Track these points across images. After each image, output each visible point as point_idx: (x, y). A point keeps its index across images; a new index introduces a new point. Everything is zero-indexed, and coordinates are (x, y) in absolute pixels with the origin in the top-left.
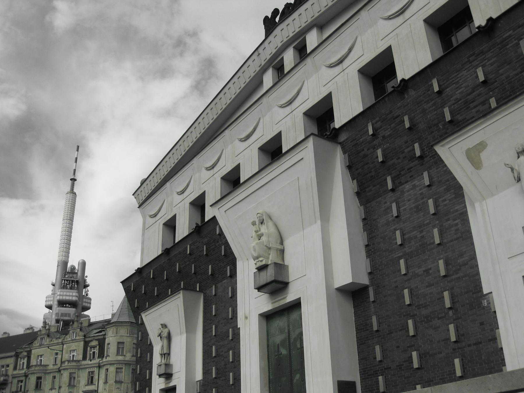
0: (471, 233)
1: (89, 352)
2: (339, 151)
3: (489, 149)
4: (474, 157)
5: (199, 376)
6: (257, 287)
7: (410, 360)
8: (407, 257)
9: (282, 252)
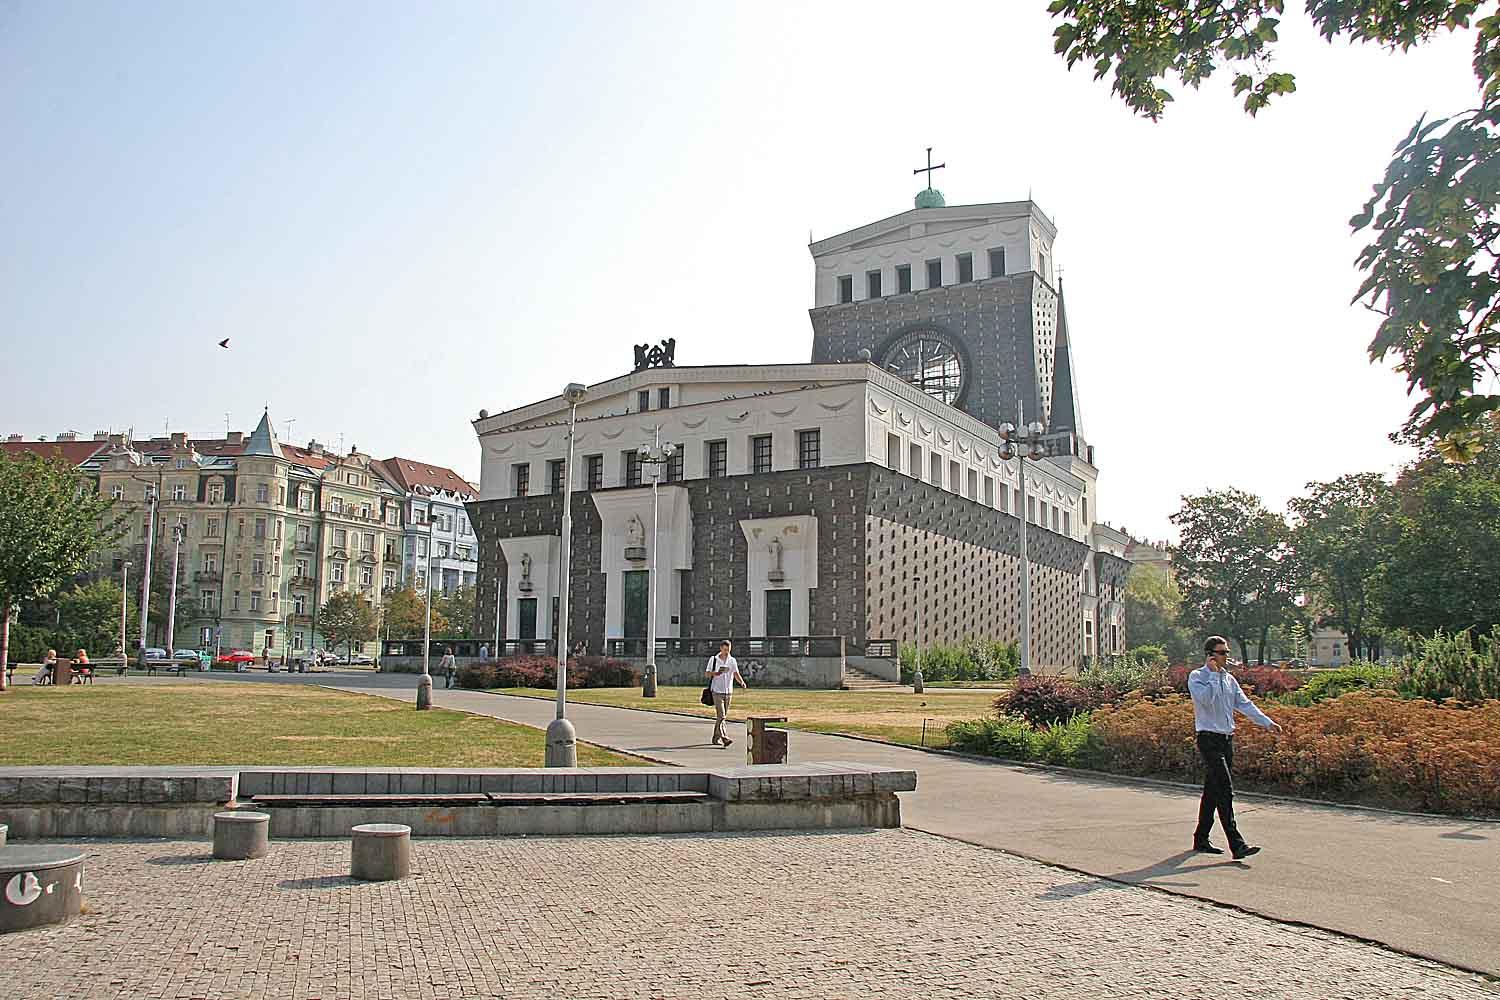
1: (209, 493)
2: (686, 490)
4: (756, 532)
9: (643, 540)
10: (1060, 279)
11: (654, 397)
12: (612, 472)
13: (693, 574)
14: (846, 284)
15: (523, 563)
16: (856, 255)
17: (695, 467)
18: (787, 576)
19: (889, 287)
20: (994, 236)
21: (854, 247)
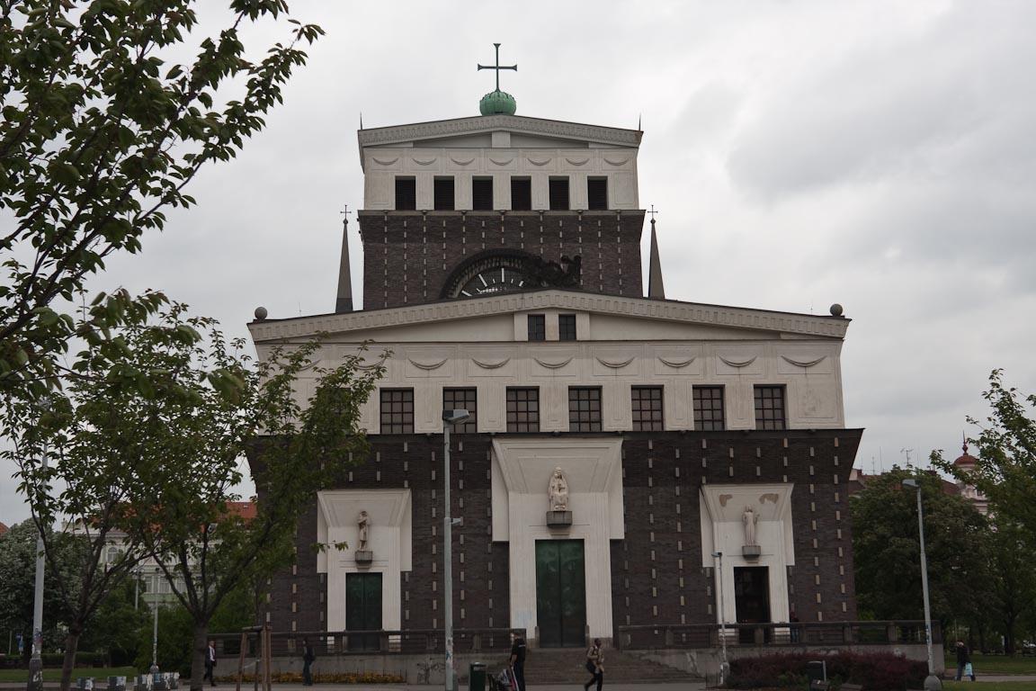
0: (700, 532)
3: (731, 500)
4: (723, 500)
5: (409, 568)
6: (550, 523)
7: (652, 591)
8: (656, 532)
10: (653, 222)
11: (552, 322)
12: (492, 415)
13: (626, 545)
14: (405, 188)
15: (362, 525)
16: (425, 155)
17: (618, 414)
18: (764, 550)
19: (464, 200)
20: (596, 163)
21: (418, 144)
